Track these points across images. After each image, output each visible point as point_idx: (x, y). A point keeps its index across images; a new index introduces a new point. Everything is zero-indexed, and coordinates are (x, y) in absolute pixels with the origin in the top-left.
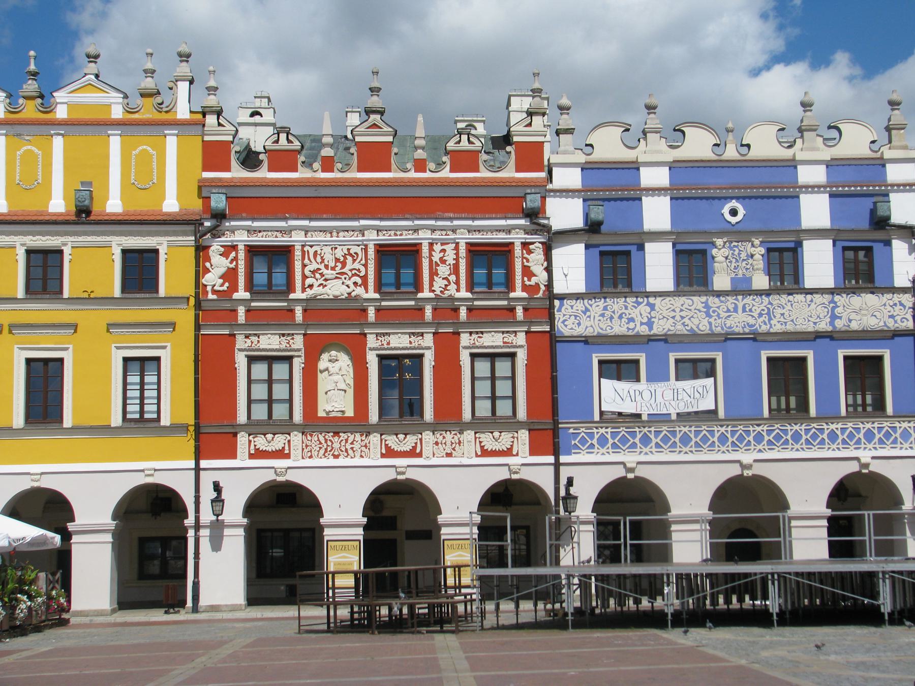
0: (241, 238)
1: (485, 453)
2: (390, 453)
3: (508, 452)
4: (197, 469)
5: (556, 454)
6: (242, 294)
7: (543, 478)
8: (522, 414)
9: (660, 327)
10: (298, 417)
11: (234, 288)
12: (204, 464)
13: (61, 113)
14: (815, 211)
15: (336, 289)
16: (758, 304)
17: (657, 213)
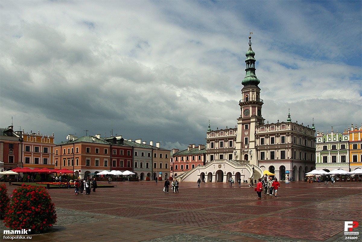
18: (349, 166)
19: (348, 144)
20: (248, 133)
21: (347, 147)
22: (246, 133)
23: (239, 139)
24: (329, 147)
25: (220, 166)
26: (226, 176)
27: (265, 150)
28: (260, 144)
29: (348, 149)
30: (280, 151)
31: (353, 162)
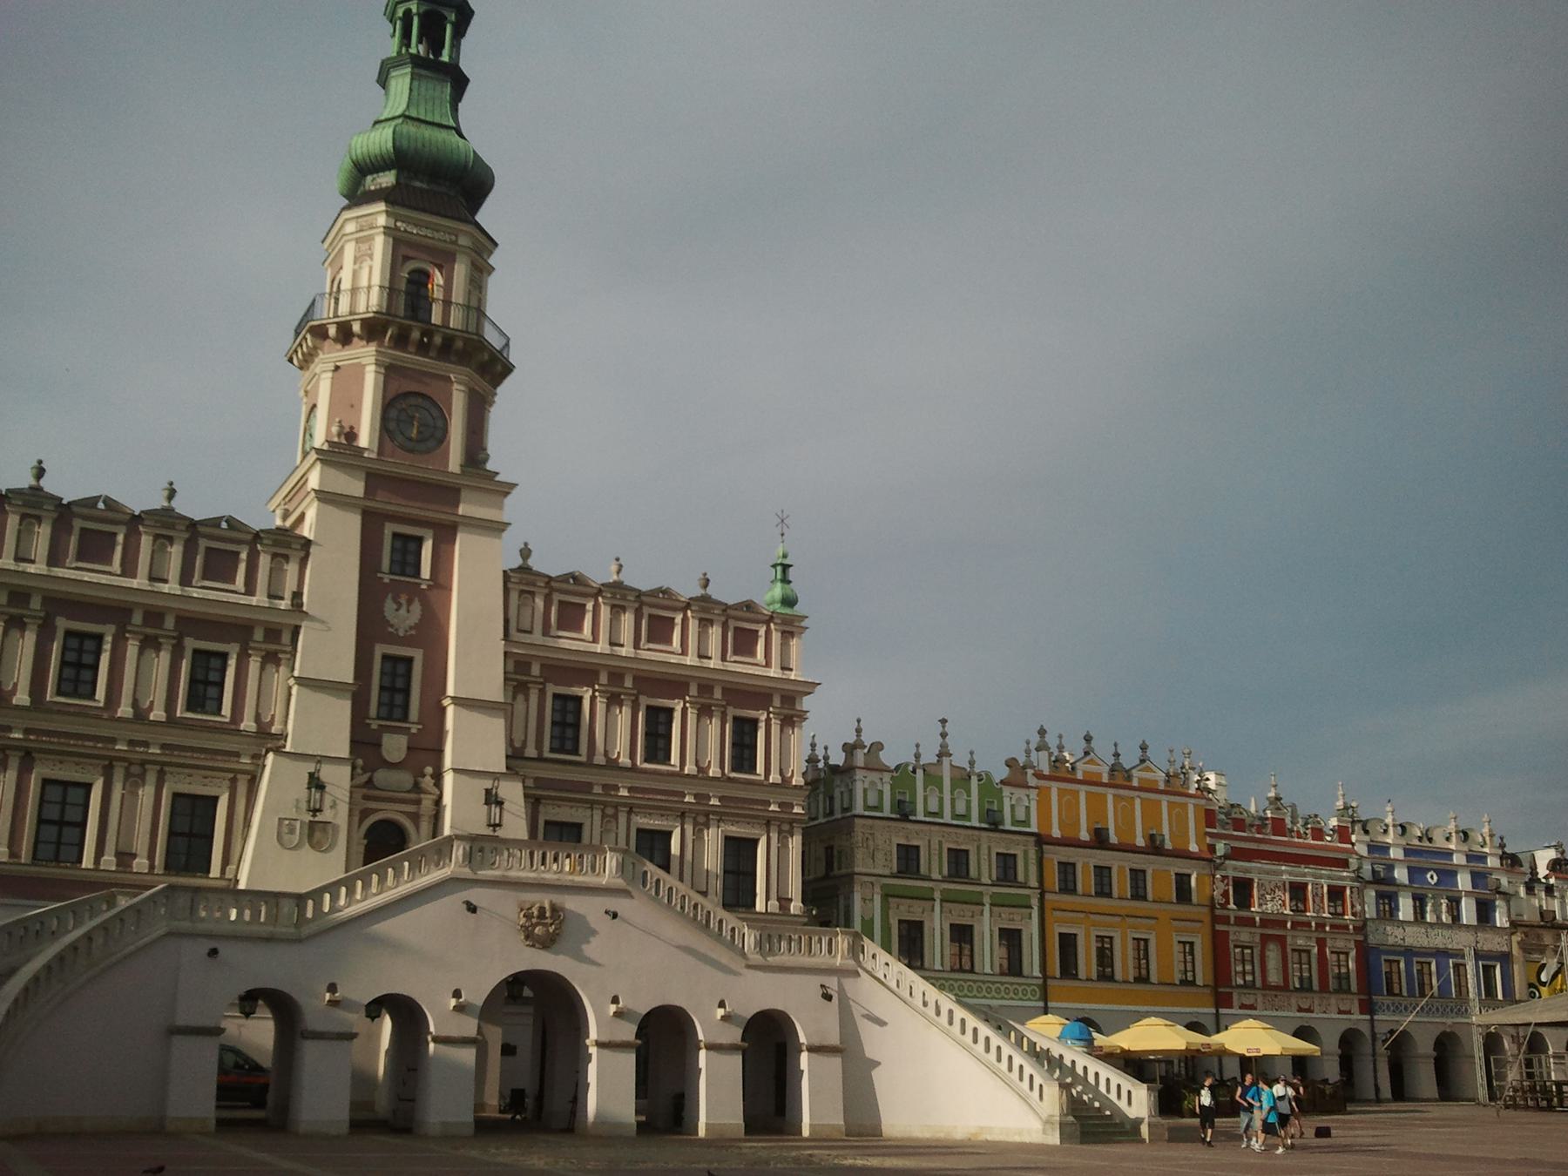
0: (1231, 873)
1: (1340, 1012)
2: (1300, 1010)
3: (1349, 1012)
4: (1217, 1014)
5: (1371, 1012)
6: (1232, 906)
7: (1365, 1029)
8: (1354, 988)
9: (1409, 941)
10: (1259, 983)
11: (1228, 902)
12: (1222, 1011)
13: (1135, 783)
14: (1464, 881)
16: (1447, 933)
17: (1400, 874)
18: (1045, 999)
19: (1032, 854)
20: (416, 608)
22: (403, 617)
23: (329, 647)
24: (934, 865)
25: (548, 928)
27: (592, 804)
29: (1036, 885)
30: (713, 839)
31: (1058, 974)
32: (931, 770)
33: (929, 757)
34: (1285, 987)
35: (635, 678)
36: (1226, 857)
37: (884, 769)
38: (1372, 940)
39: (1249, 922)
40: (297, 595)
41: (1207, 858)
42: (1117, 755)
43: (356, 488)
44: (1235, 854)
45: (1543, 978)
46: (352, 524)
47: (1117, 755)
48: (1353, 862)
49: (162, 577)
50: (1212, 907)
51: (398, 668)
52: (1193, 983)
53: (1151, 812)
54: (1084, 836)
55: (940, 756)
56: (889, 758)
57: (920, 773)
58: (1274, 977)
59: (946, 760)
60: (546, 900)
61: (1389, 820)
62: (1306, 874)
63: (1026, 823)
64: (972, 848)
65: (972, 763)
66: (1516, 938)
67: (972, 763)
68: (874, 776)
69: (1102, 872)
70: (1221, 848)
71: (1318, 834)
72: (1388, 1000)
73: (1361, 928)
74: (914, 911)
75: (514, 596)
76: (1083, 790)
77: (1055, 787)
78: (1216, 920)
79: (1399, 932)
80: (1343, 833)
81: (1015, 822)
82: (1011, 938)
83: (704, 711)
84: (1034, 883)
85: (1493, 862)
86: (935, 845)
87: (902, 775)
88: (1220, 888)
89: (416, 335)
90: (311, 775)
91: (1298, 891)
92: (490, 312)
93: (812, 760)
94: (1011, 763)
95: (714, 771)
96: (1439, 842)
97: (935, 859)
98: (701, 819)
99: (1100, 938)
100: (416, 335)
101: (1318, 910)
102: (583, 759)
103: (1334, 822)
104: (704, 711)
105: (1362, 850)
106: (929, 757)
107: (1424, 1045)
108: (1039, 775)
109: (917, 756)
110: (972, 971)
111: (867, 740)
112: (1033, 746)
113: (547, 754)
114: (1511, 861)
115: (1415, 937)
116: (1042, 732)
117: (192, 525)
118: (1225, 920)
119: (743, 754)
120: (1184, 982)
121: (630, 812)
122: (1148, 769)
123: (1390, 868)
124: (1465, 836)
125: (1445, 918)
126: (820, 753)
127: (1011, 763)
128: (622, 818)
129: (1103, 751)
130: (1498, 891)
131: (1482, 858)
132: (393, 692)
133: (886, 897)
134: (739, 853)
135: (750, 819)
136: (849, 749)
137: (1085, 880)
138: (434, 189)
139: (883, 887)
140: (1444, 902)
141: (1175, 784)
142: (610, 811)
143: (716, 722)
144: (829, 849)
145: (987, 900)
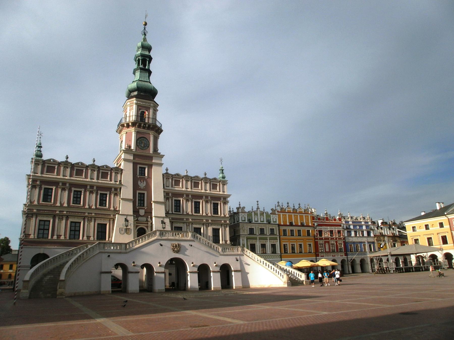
0: (318, 229)
7: (346, 259)
9: (354, 241)
14: (364, 228)
15: (326, 236)
18: (281, 258)
20: (145, 182)
21: (276, 232)
22: (142, 185)
23: (127, 192)
25: (177, 249)
26: (219, 274)
27: (184, 223)
28: (172, 211)
30: (210, 230)
32: (255, 212)
33: (255, 209)
34: (329, 252)
35: (191, 196)
36: (317, 226)
37: (246, 212)
38: (347, 241)
39: (322, 239)
40: (120, 181)
41: (313, 226)
42: (294, 206)
43: (131, 158)
44: (319, 225)
45: (381, 246)
46: (131, 165)
47: (294, 206)
48: (342, 225)
49: (92, 178)
50: (314, 237)
51: (142, 195)
52: (311, 252)
53: (301, 218)
54: (288, 224)
55: (257, 209)
56: (247, 210)
57: (253, 213)
58: (327, 250)
59: (258, 210)
60: (177, 243)
61: (349, 216)
62: (333, 228)
63: (276, 222)
64: (265, 228)
65: (264, 210)
66: (375, 239)
67: (264, 210)
68: (243, 214)
69: (292, 231)
70: (316, 224)
71: (335, 220)
72: (350, 253)
73: (344, 239)
74: (253, 242)
75: (165, 179)
76: (287, 214)
77: (281, 214)
78: (315, 239)
79: (352, 239)
80: (340, 219)
81: (273, 222)
82: (273, 246)
83: (207, 202)
84: (278, 234)
85: (370, 223)
86: (257, 228)
87: (249, 213)
88: (316, 232)
89: (142, 125)
90: (125, 219)
91: (331, 232)
92: (158, 119)
93: (230, 211)
94: (272, 210)
95: (209, 215)
96: (359, 220)
97: (257, 231)
98: (207, 225)
99: (292, 245)
100: (142, 125)
101: (336, 236)
102: (181, 213)
103: (338, 217)
104: (207, 202)
105: (344, 222)
106: (255, 209)
107: (358, 262)
108: (278, 212)
109: (252, 209)
110: (266, 253)
111: (242, 206)
112: (277, 205)
113: (174, 213)
114: (374, 223)
115: (355, 240)
116: (278, 203)
117: (99, 167)
118: (317, 239)
119: (215, 210)
120: (309, 252)
121: (192, 224)
122: (300, 209)
123: (350, 226)
124: (364, 218)
125: (361, 235)
126: (231, 210)
127: (272, 210)
128: (191, 225)
129: (291, 206)
130: (371, 229)
131: (368, 223)
132: (141, 201)
133: (247, 239)
134: (216, 232)
135: (217, 224)
136: (238, 209)
137: (288, 233)
138: (145, 95)
139: (246, 237)
140: (360, 232)
141: (306, 212)
142: (188, 224)
143: (209, 204)
144: (234, 230)
145: (268, 238)
